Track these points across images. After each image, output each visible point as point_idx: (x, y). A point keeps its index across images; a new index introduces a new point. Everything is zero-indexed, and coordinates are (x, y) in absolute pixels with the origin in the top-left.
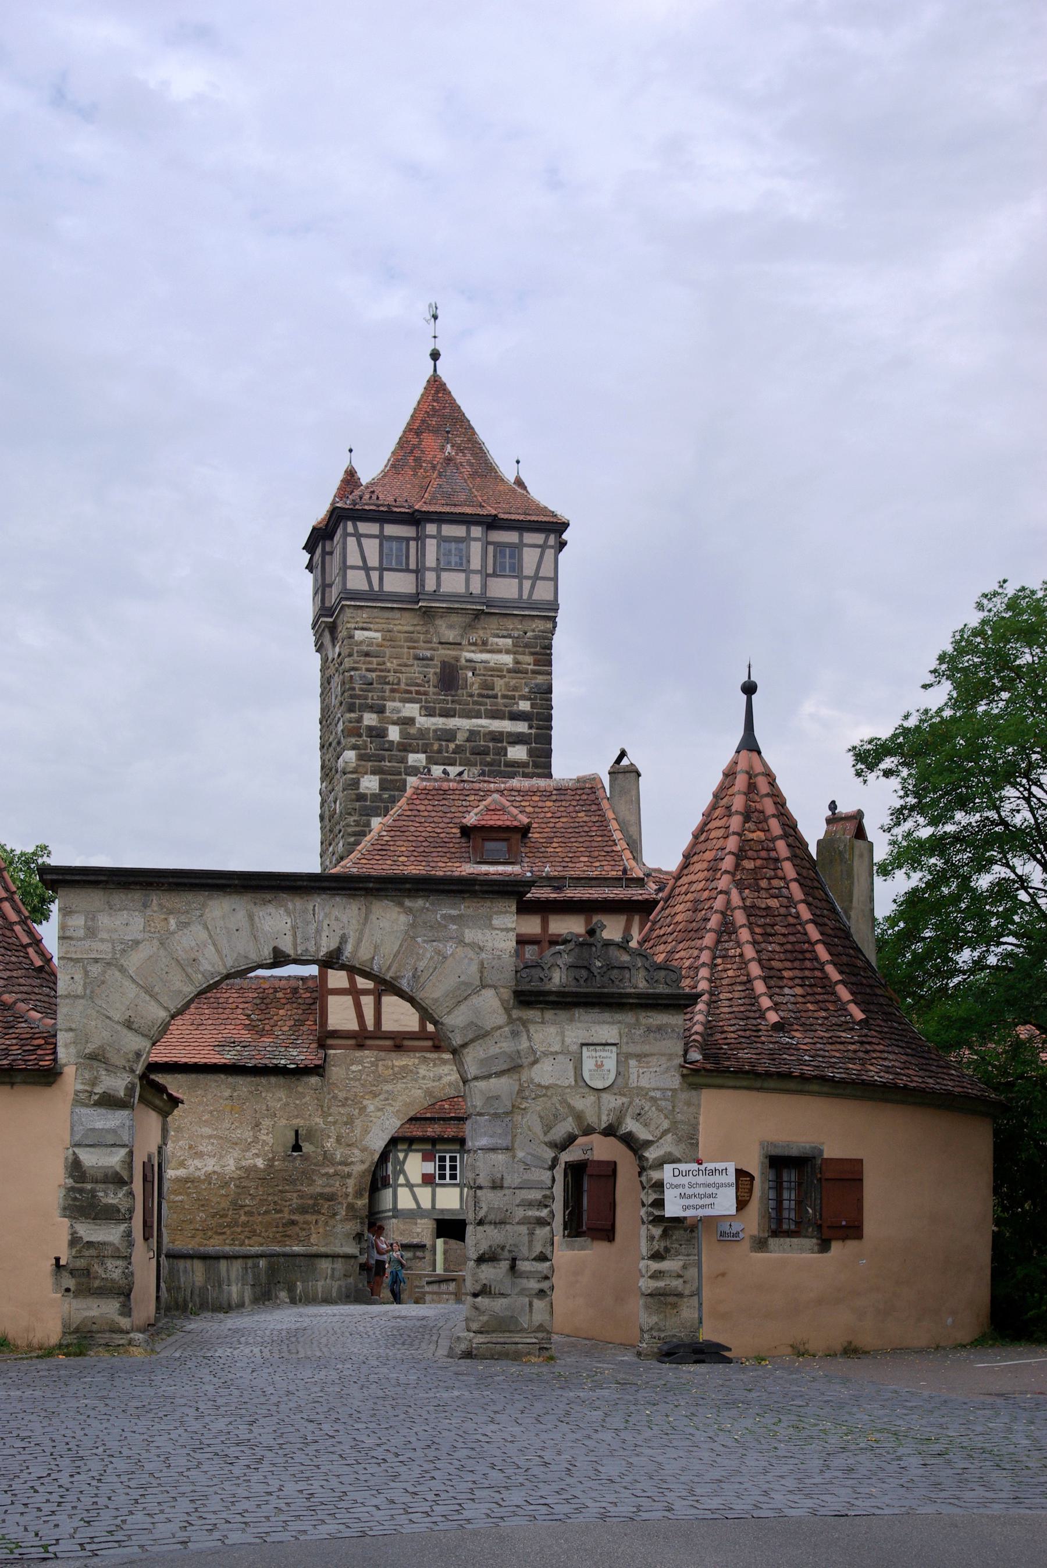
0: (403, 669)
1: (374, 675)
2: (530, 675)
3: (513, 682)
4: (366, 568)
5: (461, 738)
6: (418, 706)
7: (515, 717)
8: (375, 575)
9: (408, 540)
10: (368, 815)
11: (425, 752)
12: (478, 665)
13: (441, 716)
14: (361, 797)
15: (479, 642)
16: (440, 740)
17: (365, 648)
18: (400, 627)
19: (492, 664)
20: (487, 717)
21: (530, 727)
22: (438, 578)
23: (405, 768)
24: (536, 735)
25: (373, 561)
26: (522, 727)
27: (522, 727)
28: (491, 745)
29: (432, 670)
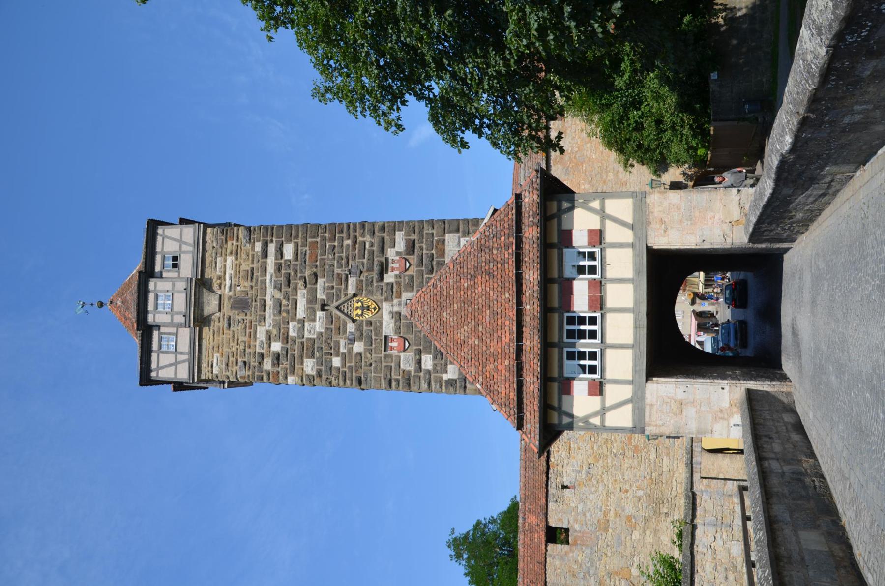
0: (236, 338)
1: (240, 360)
2: (239, 244)
3: (244, 256)
4: (176, 364)
5: (278, 295)
6: (258, 328)
7: (265, 255)
8: (181, 358)
9: (160, 333)
10: (331, 369)
11: (288, 323)
12: (233, 283)
13: (264, 310)
14: (319, 374)
15: (219, 281)
16: (280, 311)
17: (224, 366)
18: (211, 340)
19: (232, 272)
20: (265, 276)
21: (272, 241)
22: (177, 313)
23: (299, 338)
24: (277, 237)
25: (171, 358)
26: (272, 248)
27: (272, 248)
28: (283, 272)
29: (237, 317)
